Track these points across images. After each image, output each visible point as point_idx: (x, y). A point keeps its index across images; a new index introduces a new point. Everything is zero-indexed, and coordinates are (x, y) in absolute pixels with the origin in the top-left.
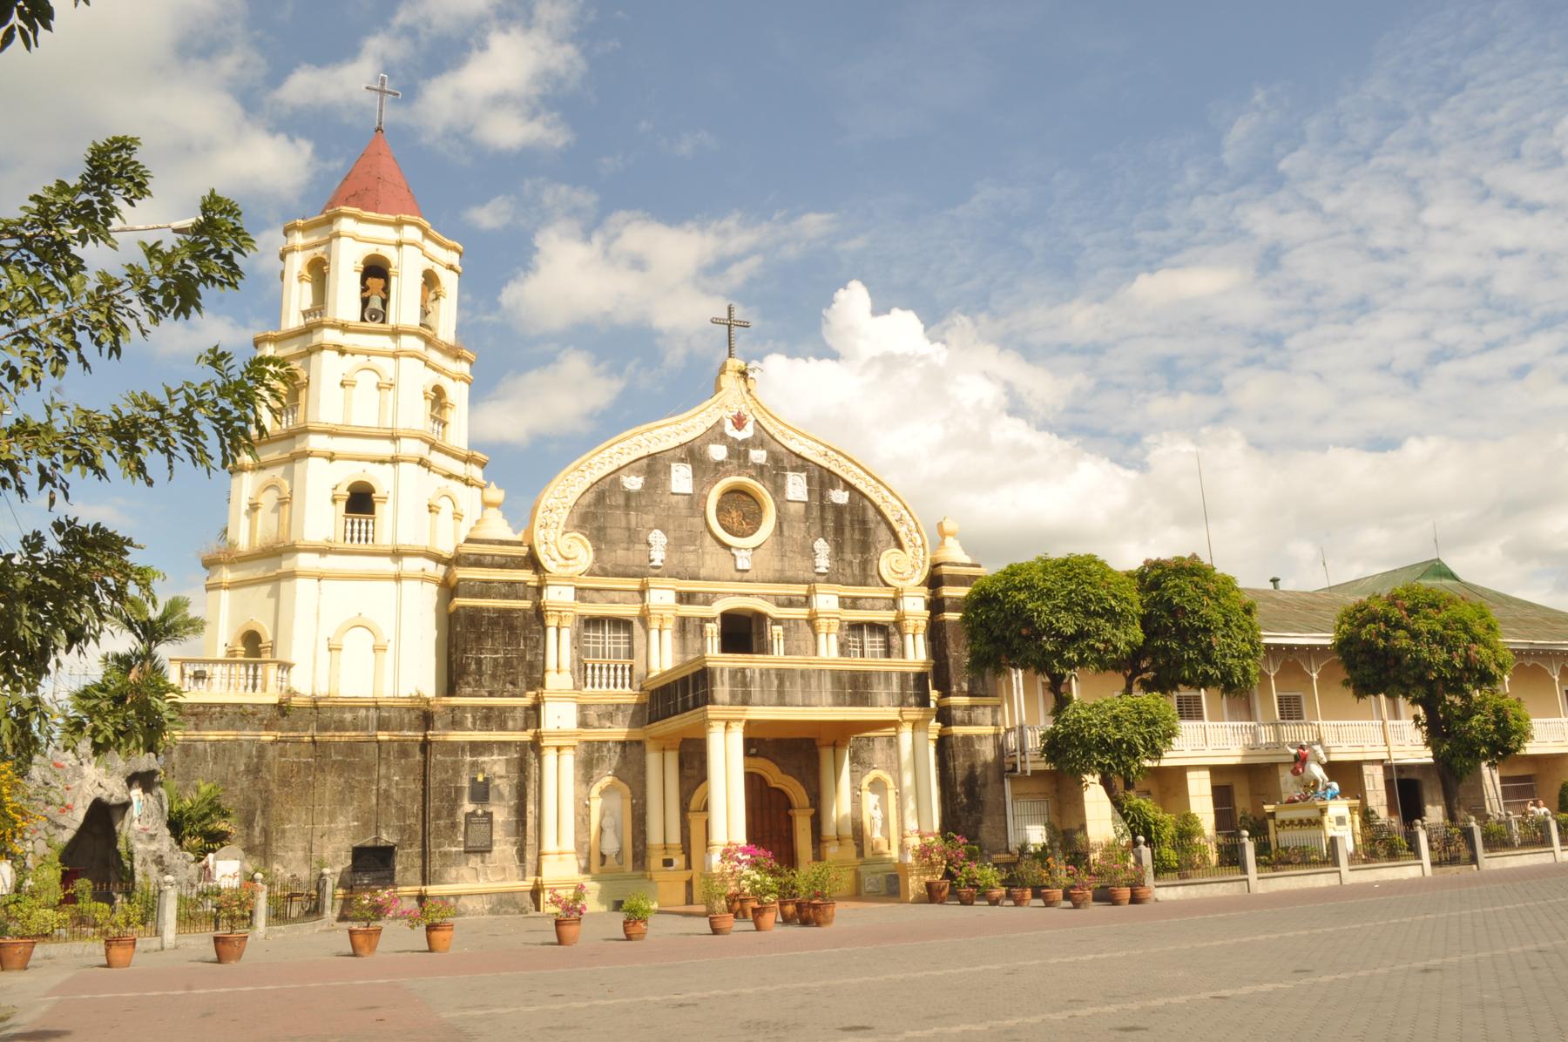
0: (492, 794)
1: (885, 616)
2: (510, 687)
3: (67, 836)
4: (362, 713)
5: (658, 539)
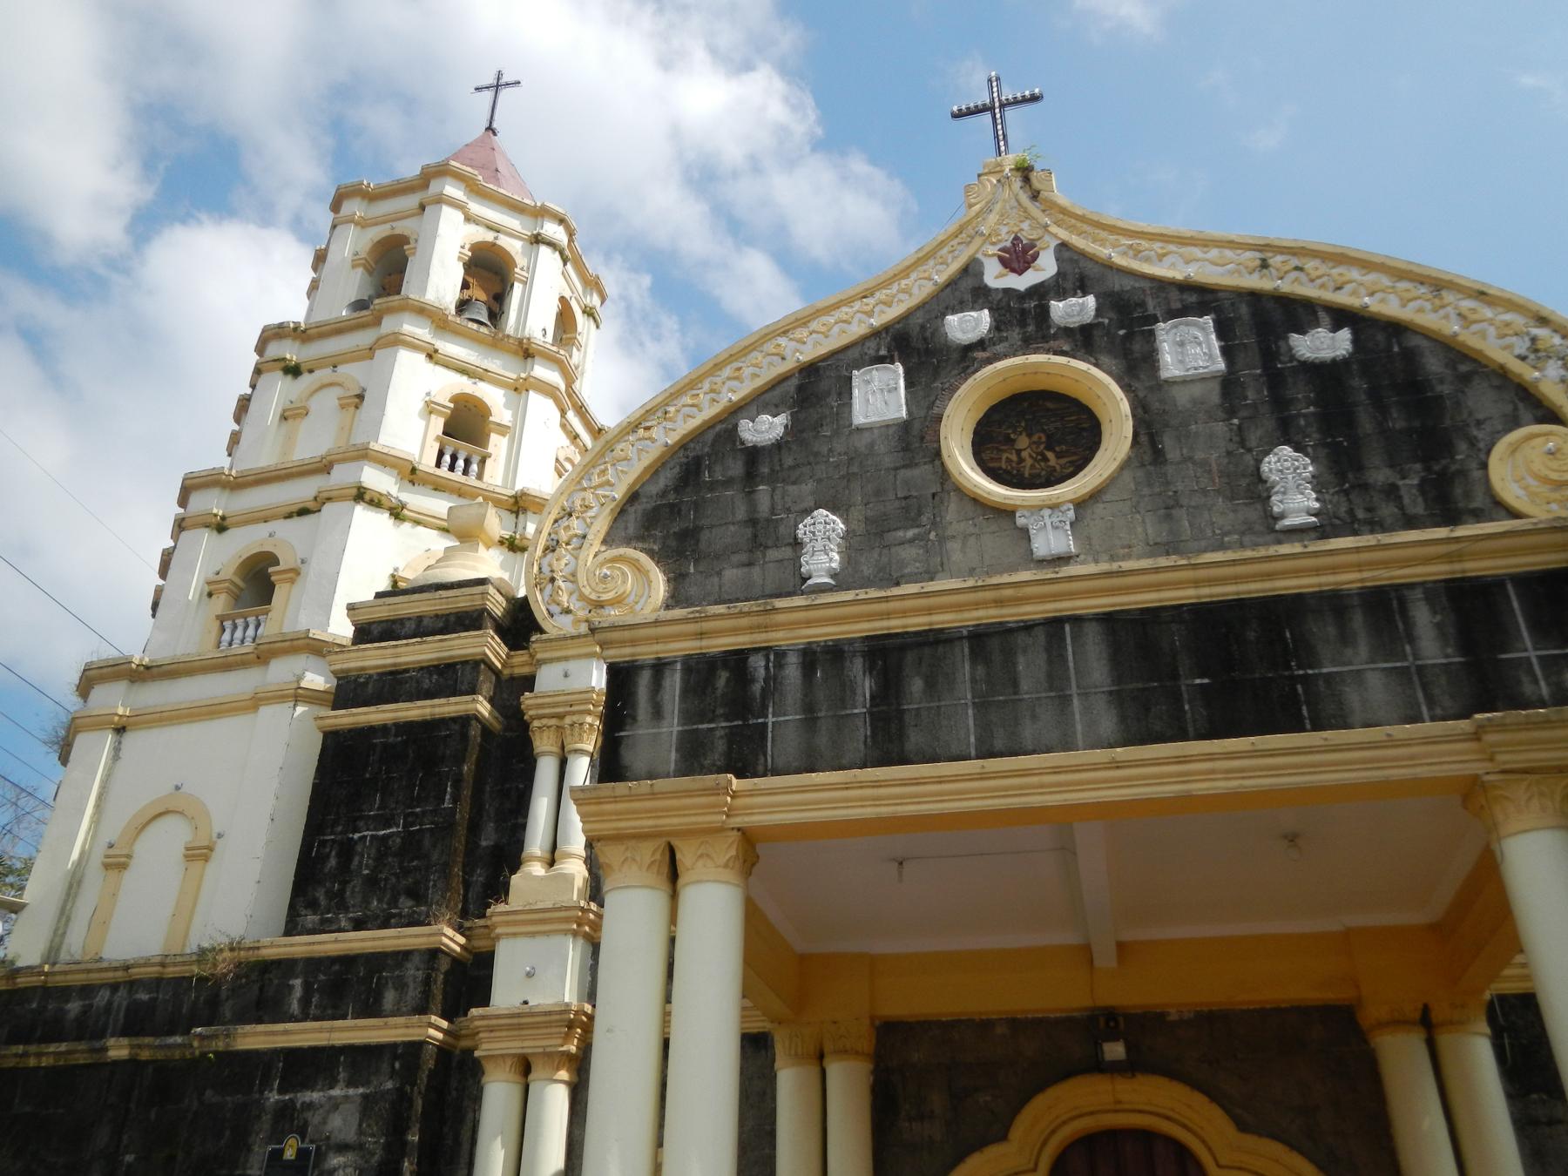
2: (406, 904)
4: (102, 998)
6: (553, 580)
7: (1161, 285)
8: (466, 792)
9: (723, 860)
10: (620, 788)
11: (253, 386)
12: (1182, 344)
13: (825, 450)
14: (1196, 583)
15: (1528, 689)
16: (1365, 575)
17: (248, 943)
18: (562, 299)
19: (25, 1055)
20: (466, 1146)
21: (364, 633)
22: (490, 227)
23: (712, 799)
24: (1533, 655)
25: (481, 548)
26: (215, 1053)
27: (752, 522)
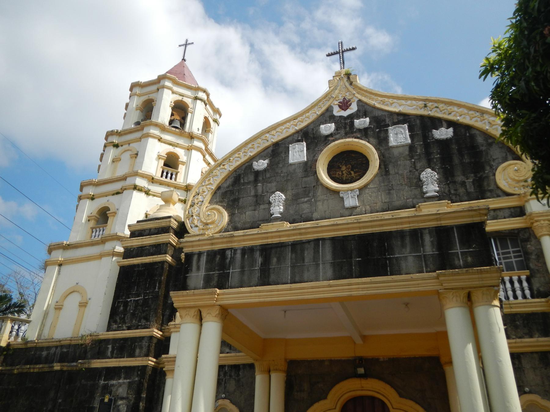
2: (143, 322)
6: (192, 216)
8: (163, 286)
9: (214, 315)
10: (185, 292)
11: (104, 151)
12: (397, 134)
13: (280, 171)
14: (360, 228)
15: (456, 262)
16: (411, 225)
17: (95, 334)
18: (206, 118)
19: (30, 368)
20: (161, 398)
21: (134, 234)
22: (181, 95)
23: (211, 296)
24: (459, 251)
25: (171, 205)
26: (85, 368)
27: (256, 196)
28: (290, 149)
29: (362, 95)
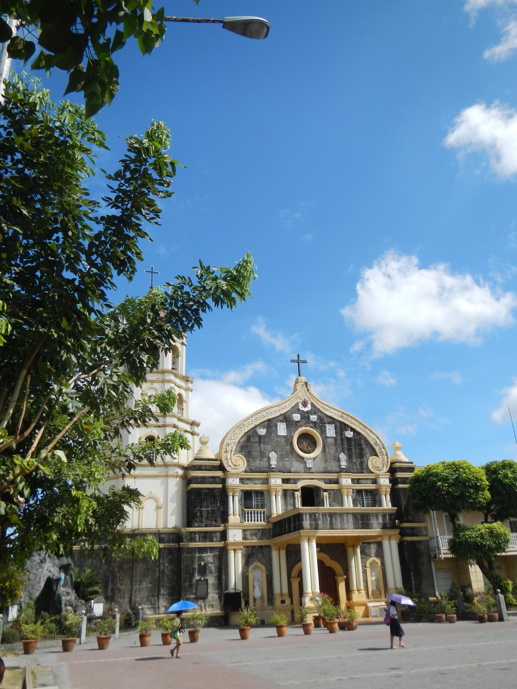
0: (208, 571)
1: (372, 487)
2: (214, 523)
3: (37, 594)
5: (273, 455)
7: (327, 416)
28: (278, 425)
29: (314, 400)
